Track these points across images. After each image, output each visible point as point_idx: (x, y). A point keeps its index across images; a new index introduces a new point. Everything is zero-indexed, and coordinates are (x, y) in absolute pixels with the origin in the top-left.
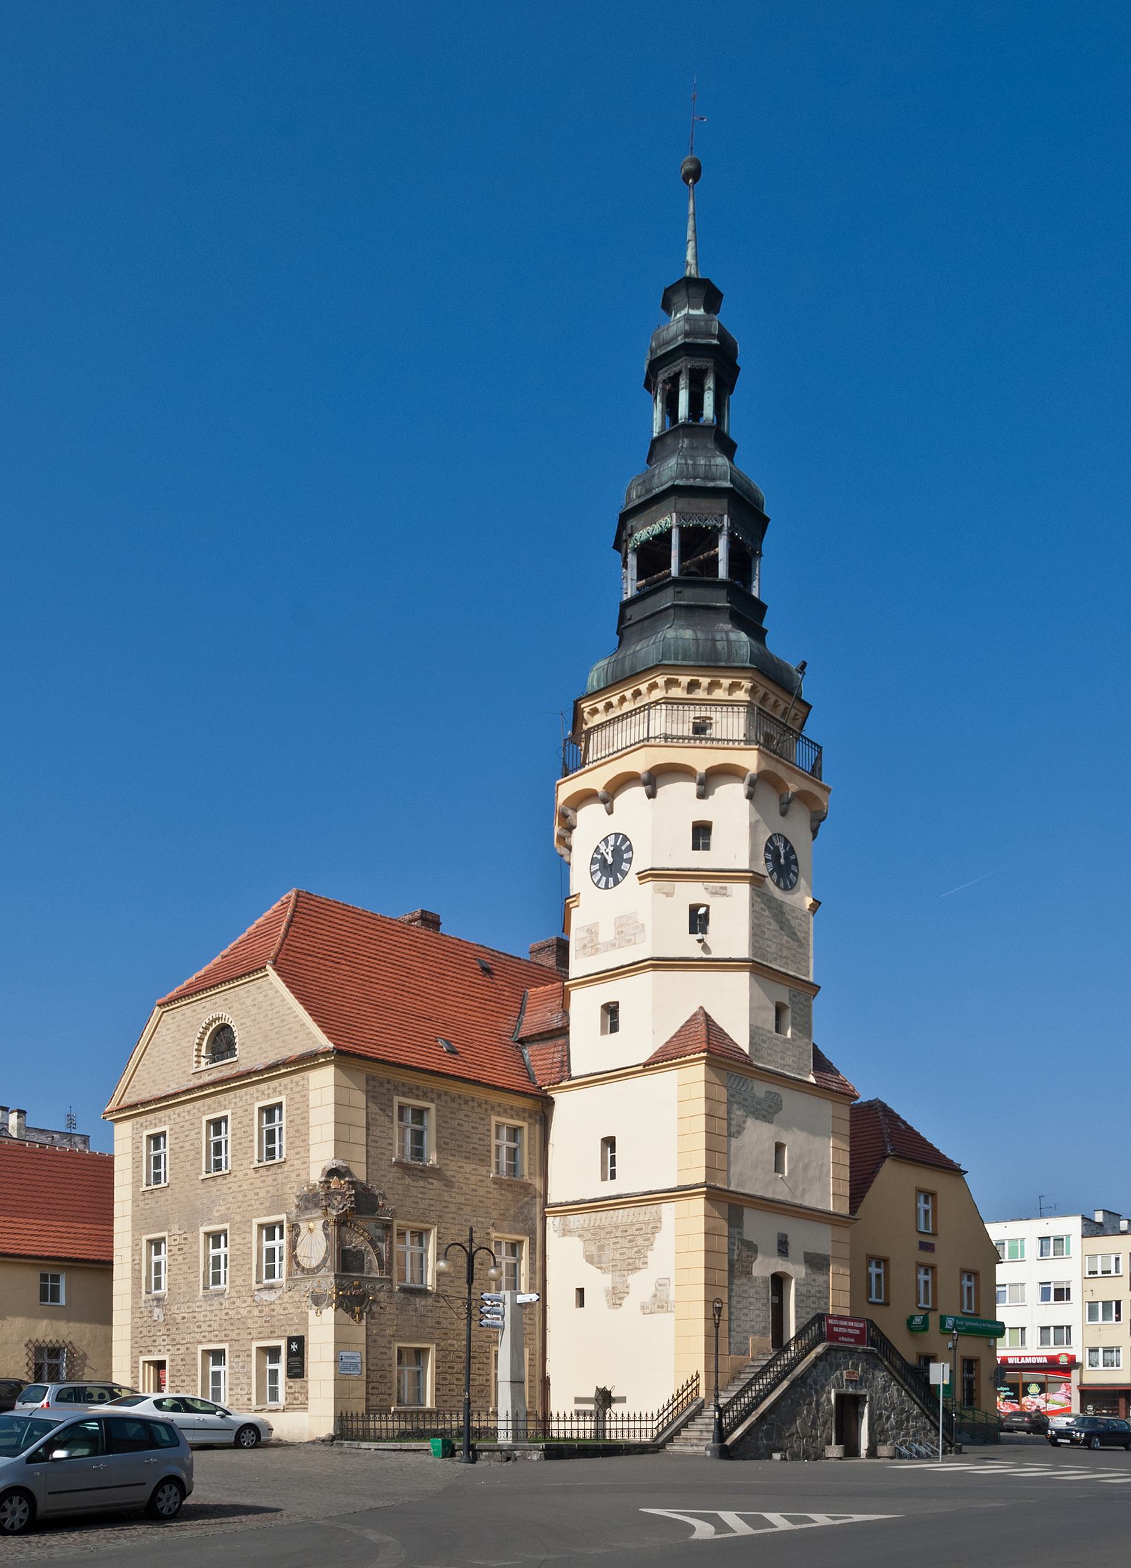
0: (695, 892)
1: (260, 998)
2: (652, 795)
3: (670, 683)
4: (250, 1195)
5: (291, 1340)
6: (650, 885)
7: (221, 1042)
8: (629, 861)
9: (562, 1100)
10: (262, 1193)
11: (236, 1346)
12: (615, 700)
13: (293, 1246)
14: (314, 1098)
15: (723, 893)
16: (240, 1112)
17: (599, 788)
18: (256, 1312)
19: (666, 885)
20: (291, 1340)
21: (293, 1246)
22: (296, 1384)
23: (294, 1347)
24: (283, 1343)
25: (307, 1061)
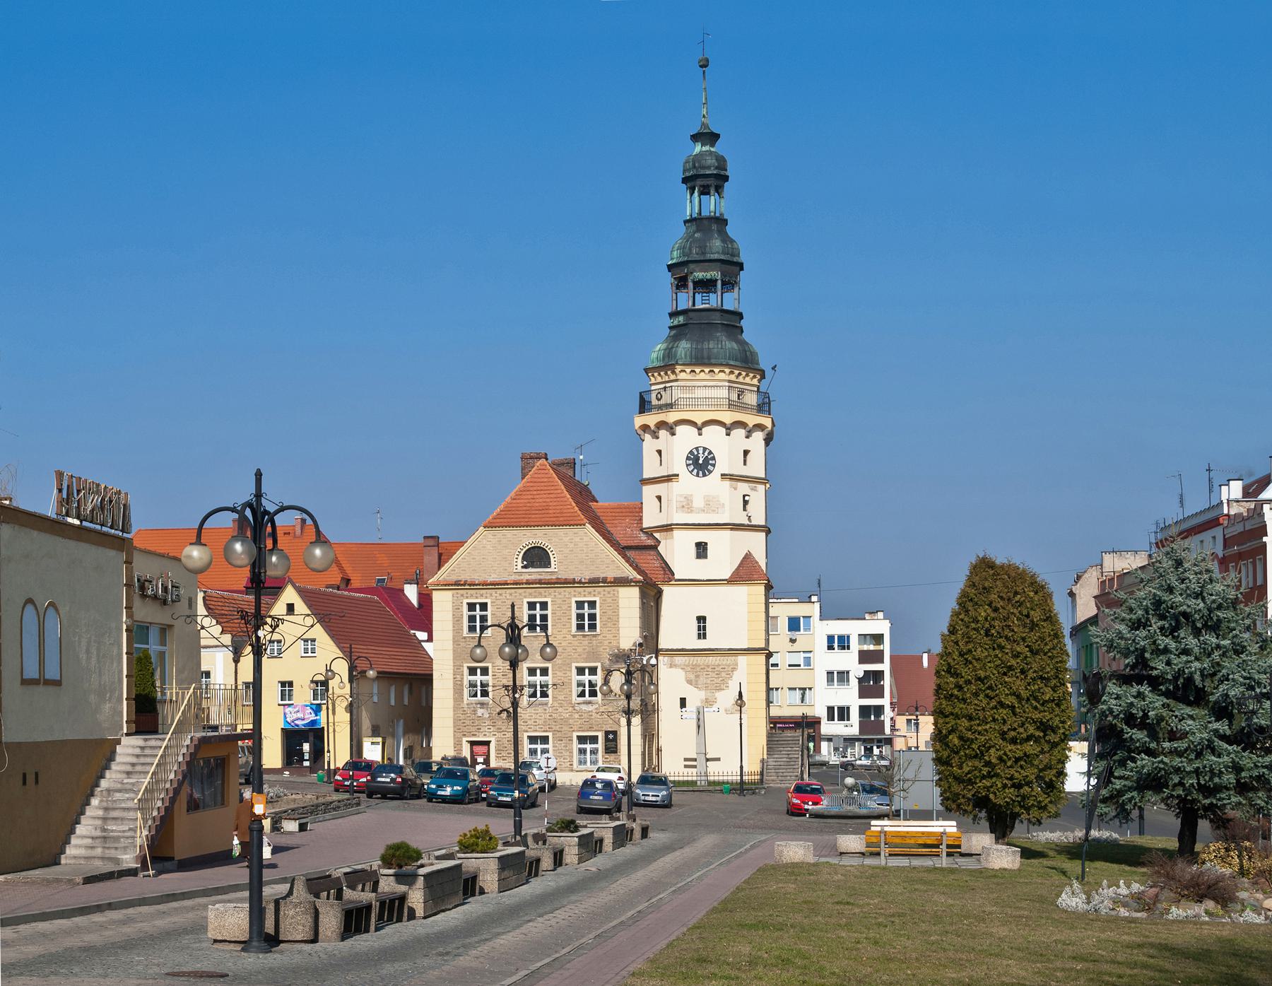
0: (744, 488)
1: (577, 539)
2: (728, 434)
3: (732, 373)
4: (569, 649)
5: (607, 733)
6: (727, 483)
7: (536, 557)
8: (714, 465)
9: (669, 592)
10: (580, 650)
11: (559, 734)
12: (697, 370)
13: (606, 682)
14: (622, 603)
15: (754, 489)
16: (559, 601)
17: (699, 423)
18: (577, 716)
19: (734, 483)
20: (607, 733)
21: (606, 682)
22: (612, 757)
23: (611, 736)
24: (601, 735)
25: (623, 582)
